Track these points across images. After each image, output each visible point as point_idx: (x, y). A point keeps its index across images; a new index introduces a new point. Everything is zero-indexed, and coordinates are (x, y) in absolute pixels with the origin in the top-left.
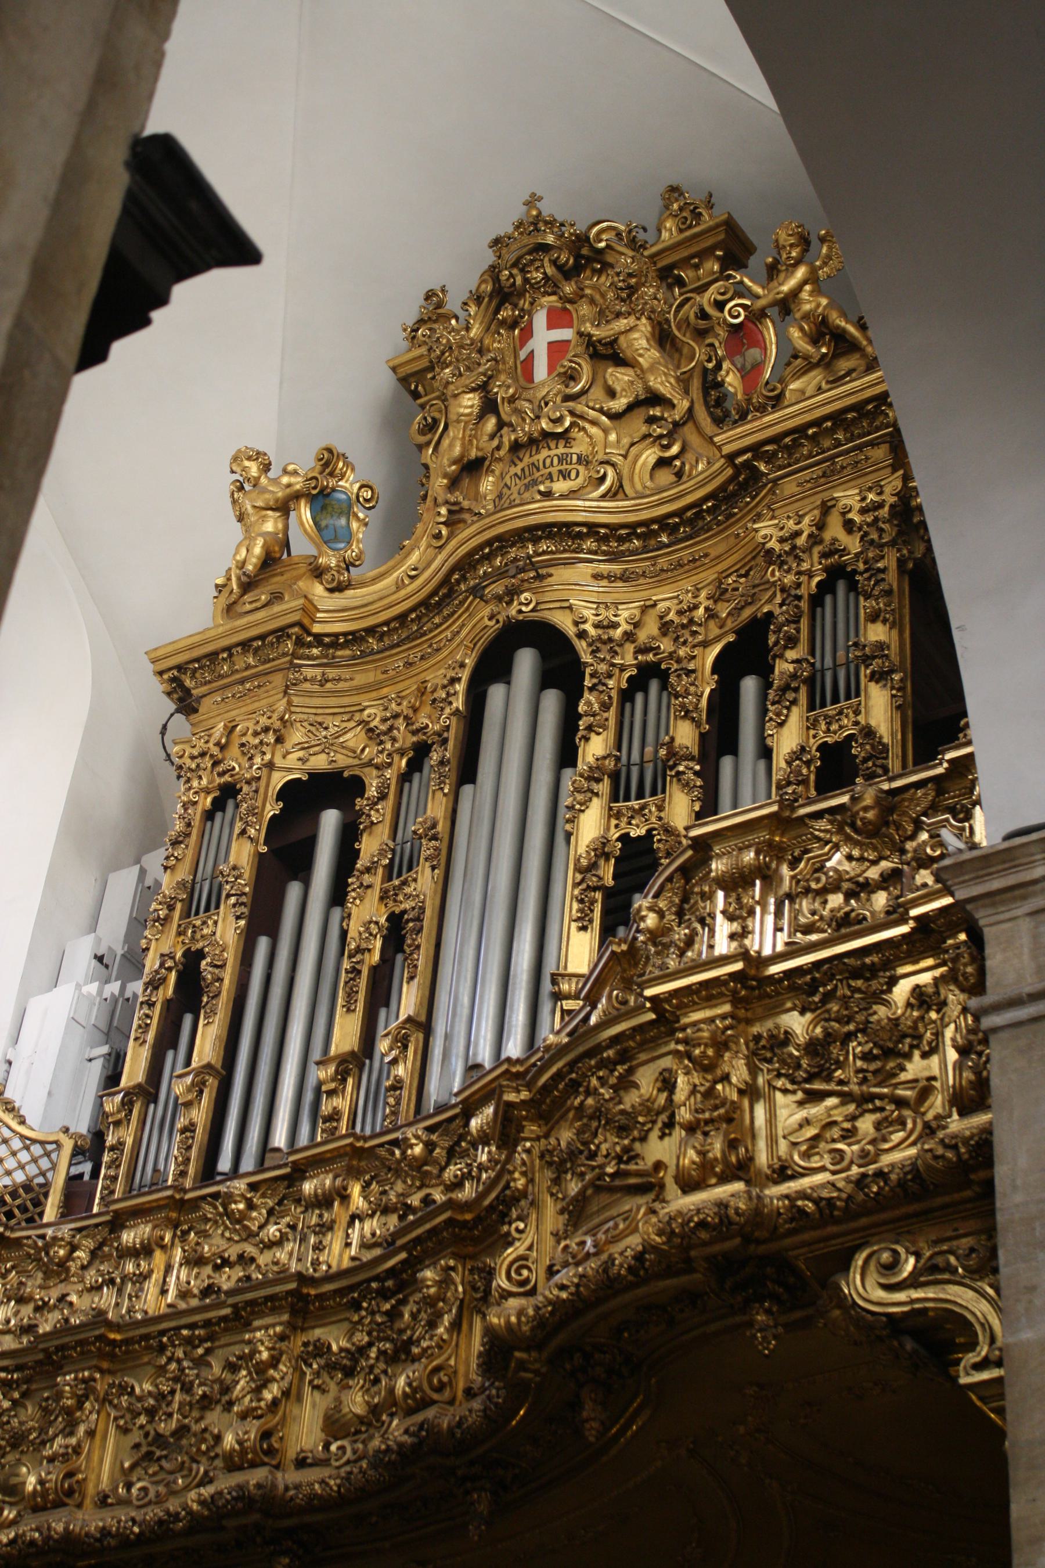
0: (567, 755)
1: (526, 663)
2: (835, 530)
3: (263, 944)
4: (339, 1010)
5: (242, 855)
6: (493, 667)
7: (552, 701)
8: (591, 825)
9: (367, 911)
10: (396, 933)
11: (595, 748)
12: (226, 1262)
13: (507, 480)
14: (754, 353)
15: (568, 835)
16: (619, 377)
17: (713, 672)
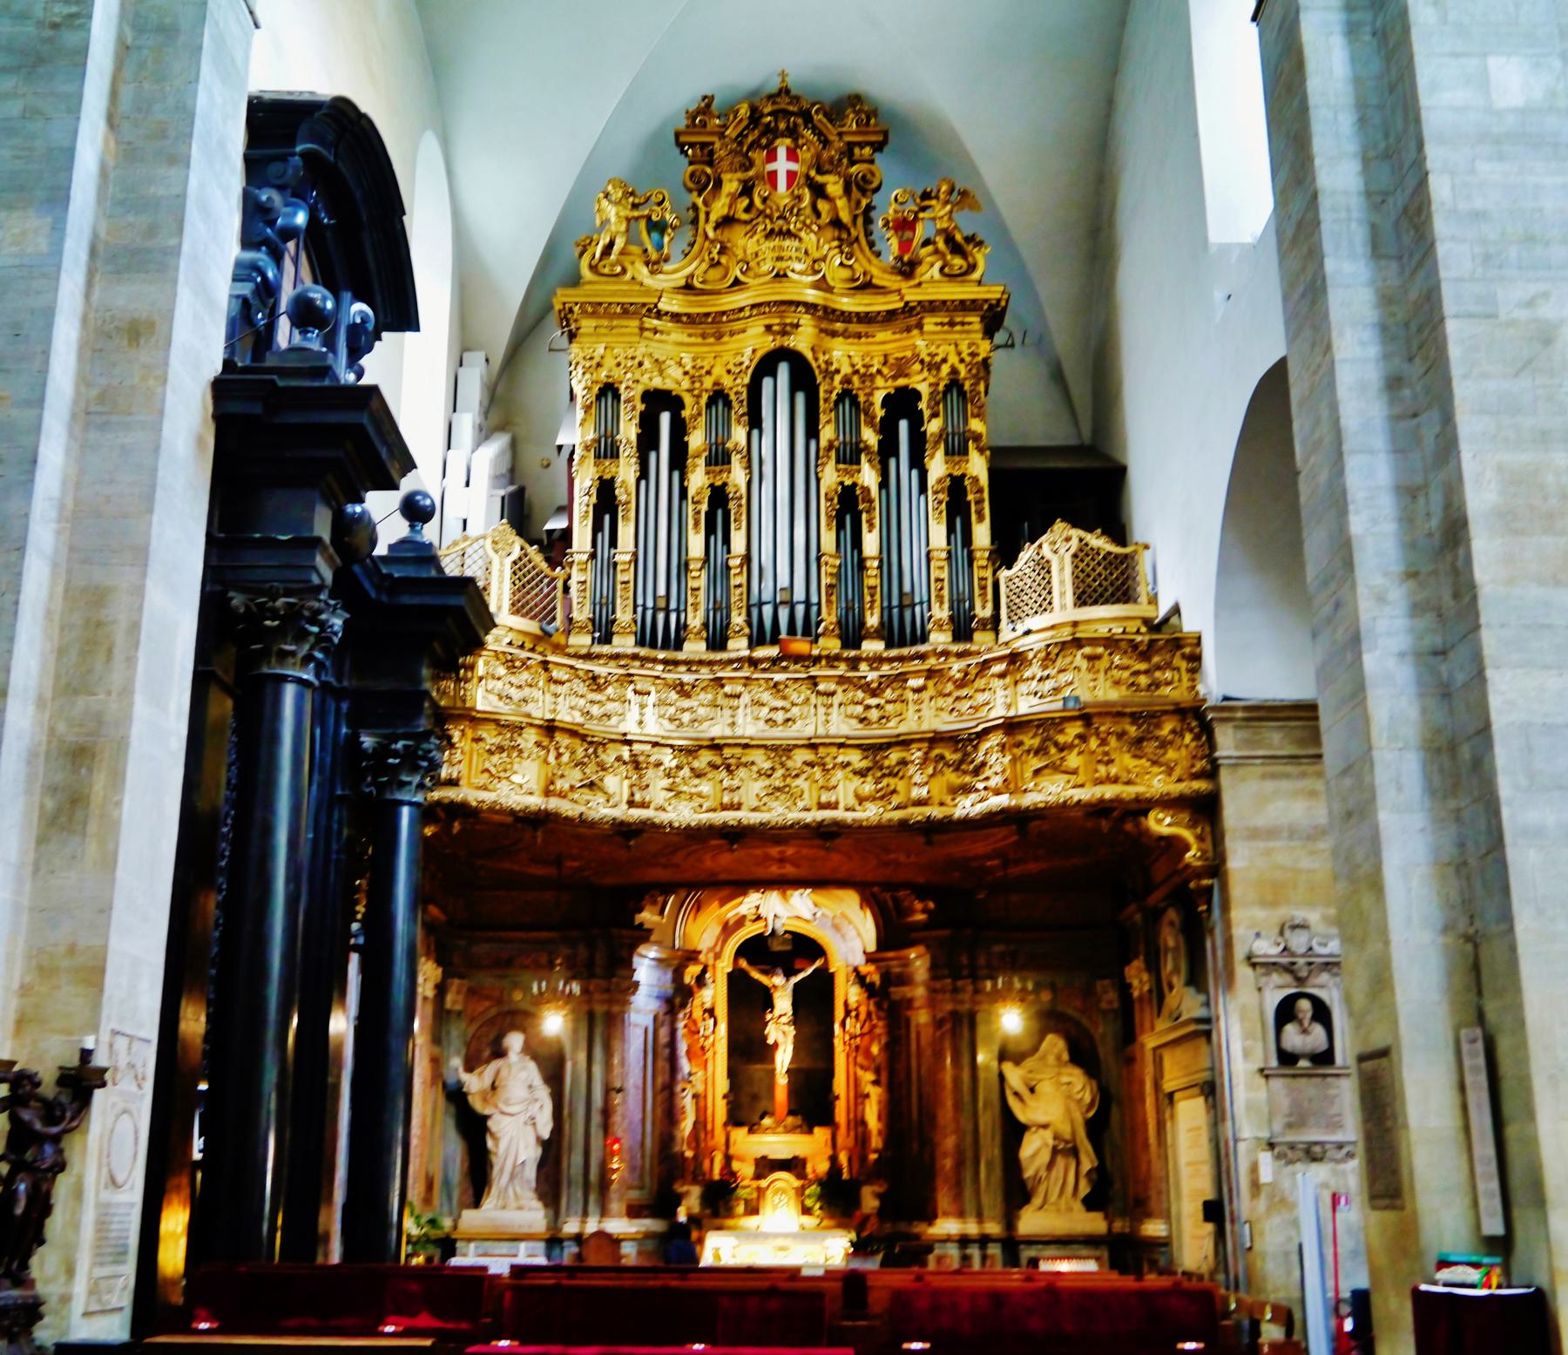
0: (812, 432)
1: (783, 370)
2: (953, 359)
3: (643, 483)
4: (691, 532)
5: (629, 431)
6: (766, 366)
7: (800, 398)
8: (830, 477)
9: (698, 479)
10: (719, 497)
11: (827, 433)
12: (776, 709)
13: (763, 247)
14: (908, 234)
15: (818, 480)
16: (823, 206)
17: (883, 406)
